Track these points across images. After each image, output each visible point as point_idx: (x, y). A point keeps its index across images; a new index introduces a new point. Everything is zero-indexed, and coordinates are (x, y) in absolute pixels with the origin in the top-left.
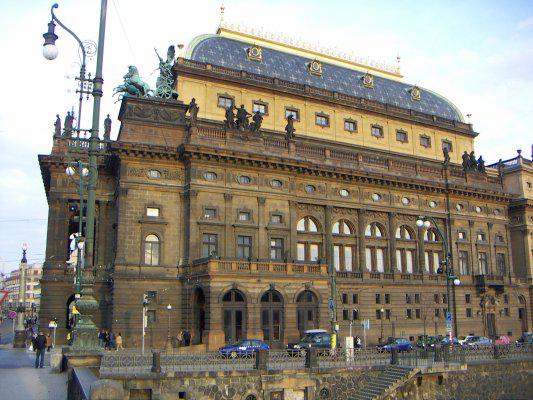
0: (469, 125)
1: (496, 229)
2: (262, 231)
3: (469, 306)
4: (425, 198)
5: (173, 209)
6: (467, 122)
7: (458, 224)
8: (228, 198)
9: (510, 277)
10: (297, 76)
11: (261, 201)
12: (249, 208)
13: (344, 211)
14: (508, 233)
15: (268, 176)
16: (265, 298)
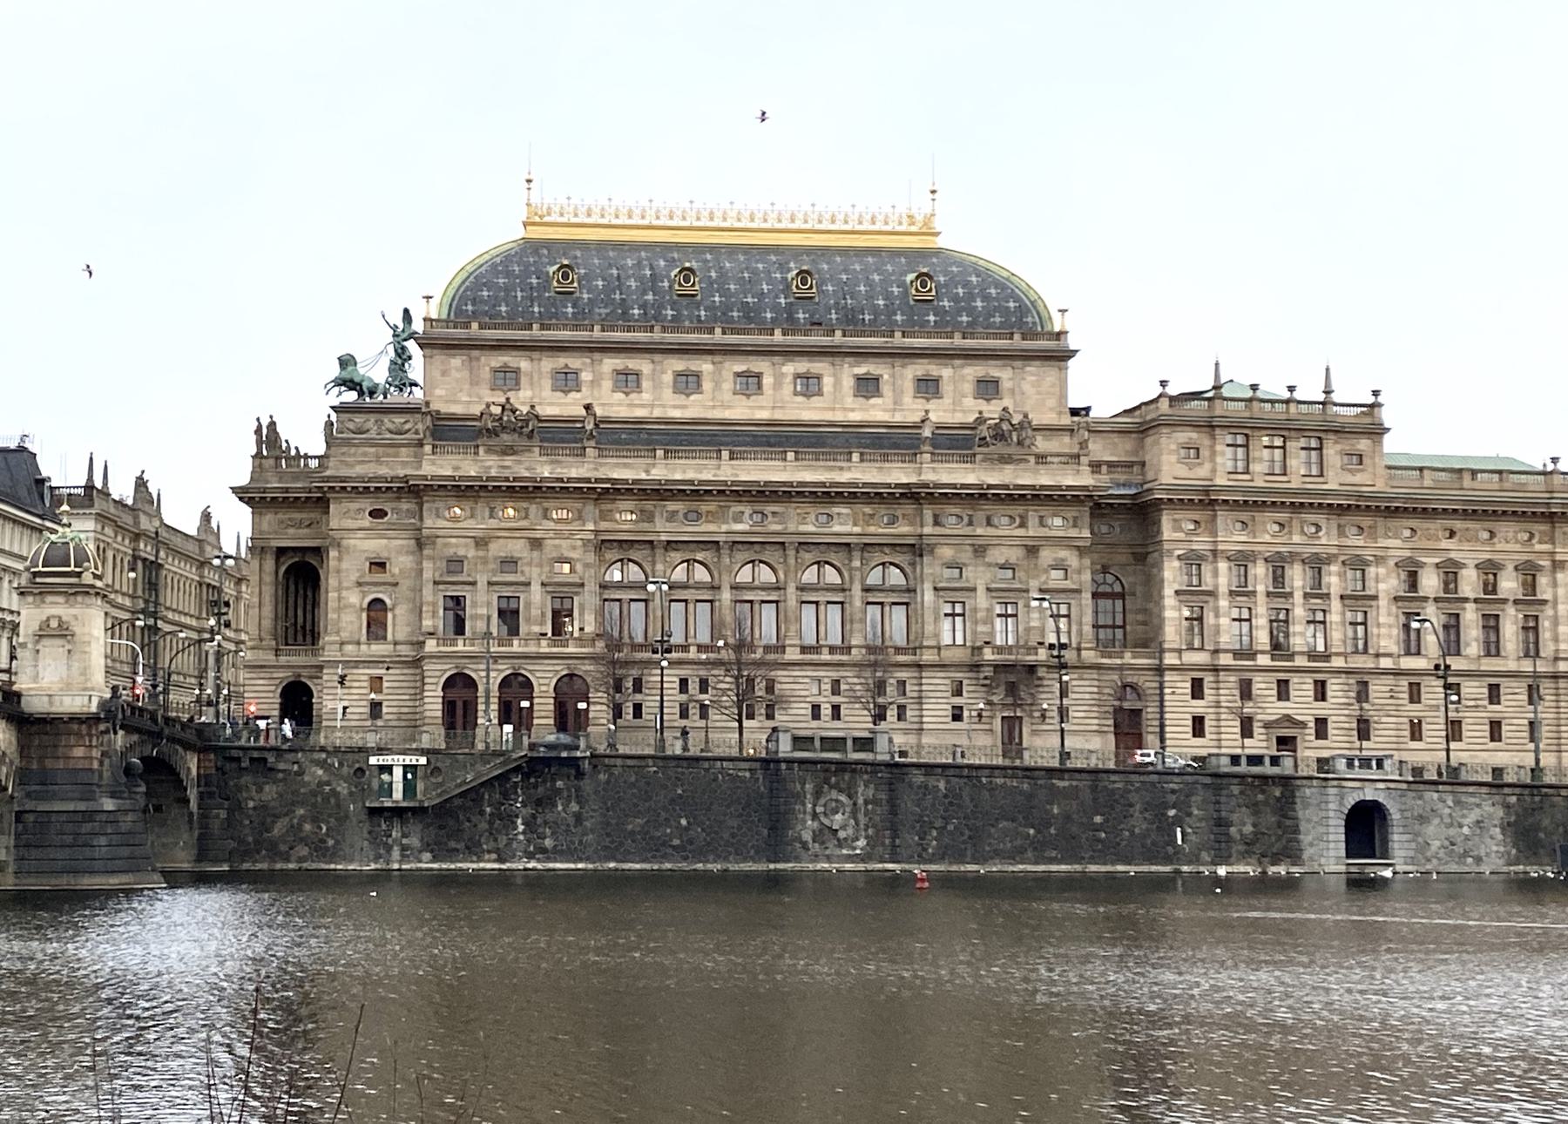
0: (1059, 335)
1: (1047, 555)
2: (536, 588)
3: (957, 701)
4: (868, 510)
5: (401, 563)
6: (1057, 329)
7: (946, 553)
8: (481, 542)
9: (1079, 649)
10: (643, 306)
11: (536, 544)
12: (516, 555)
13: (693, 546)
14: (1087, 562)
15: (546, 505)
16: (505, 683)
